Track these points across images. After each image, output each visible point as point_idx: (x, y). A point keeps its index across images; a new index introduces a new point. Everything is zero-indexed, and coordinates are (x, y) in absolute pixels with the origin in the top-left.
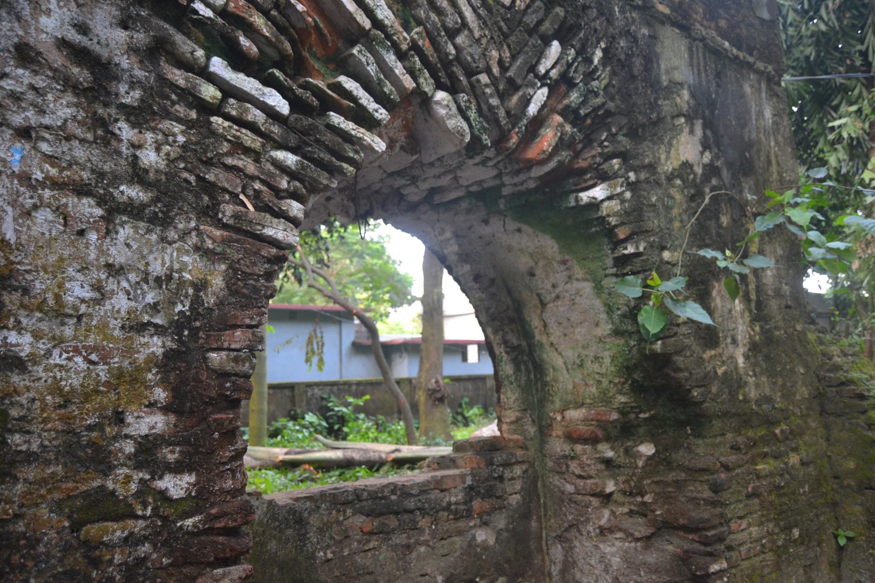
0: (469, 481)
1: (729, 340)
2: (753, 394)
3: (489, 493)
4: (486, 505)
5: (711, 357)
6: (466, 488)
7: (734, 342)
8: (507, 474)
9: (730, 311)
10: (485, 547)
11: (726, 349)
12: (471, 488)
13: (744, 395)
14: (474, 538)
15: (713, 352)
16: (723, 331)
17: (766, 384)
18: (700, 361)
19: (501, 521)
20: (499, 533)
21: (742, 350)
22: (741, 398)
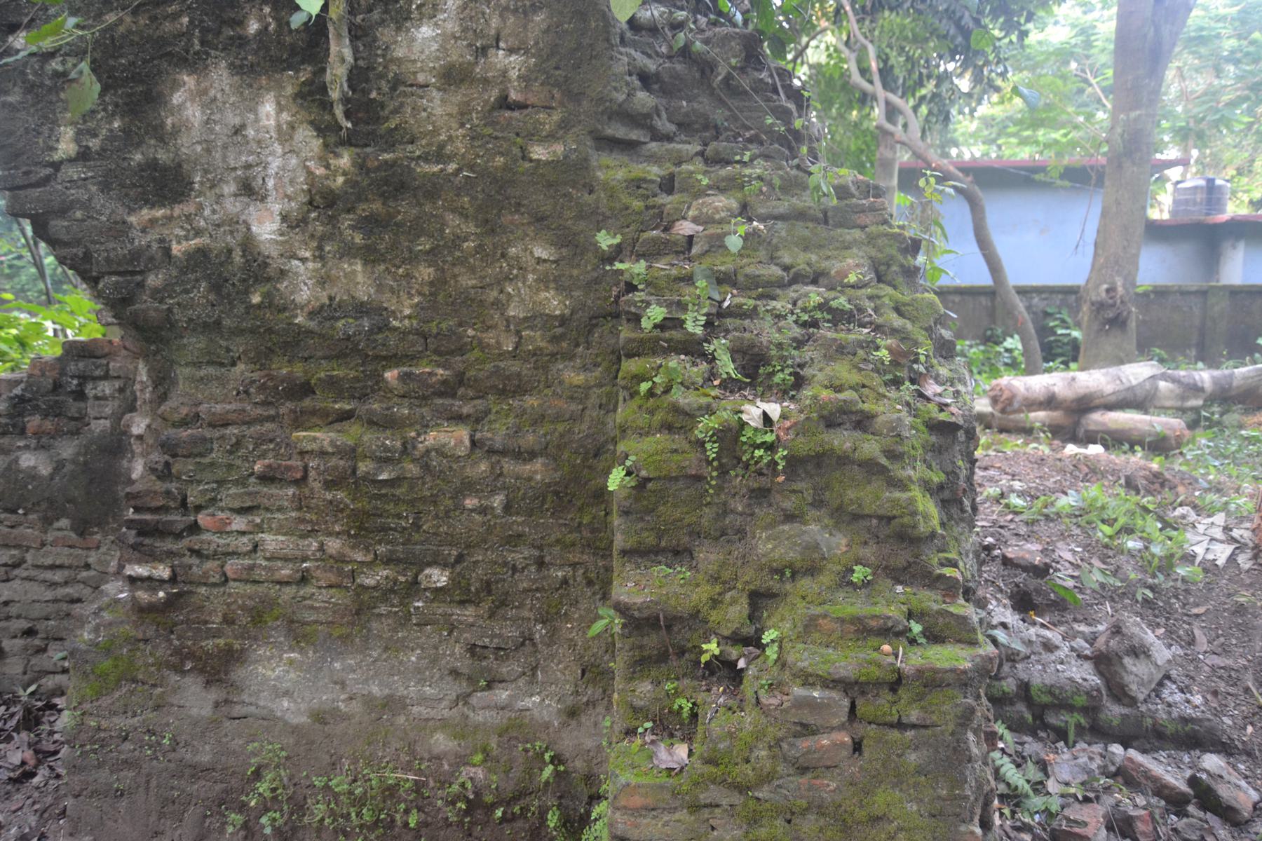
0: (18, 391)
1: (229, 188)
2: (304, 294)
3: (55, 411)
4: (49, 425)
5: (153, 222)
6: (11, 398)
7: (249, 190)
8: (90, 390)
9: (238, 130)
10: (32, 475)
11: (213, 206)
12: (21, 399)
13: (267, 295)
14: (16, 460)
15: (159, 213)
16: (206, 172)
17: (360, 278)
18: (120, 230)
19: (67, 449)
20: (59, 466)
21: (277, 208)
22: (256, 299)
